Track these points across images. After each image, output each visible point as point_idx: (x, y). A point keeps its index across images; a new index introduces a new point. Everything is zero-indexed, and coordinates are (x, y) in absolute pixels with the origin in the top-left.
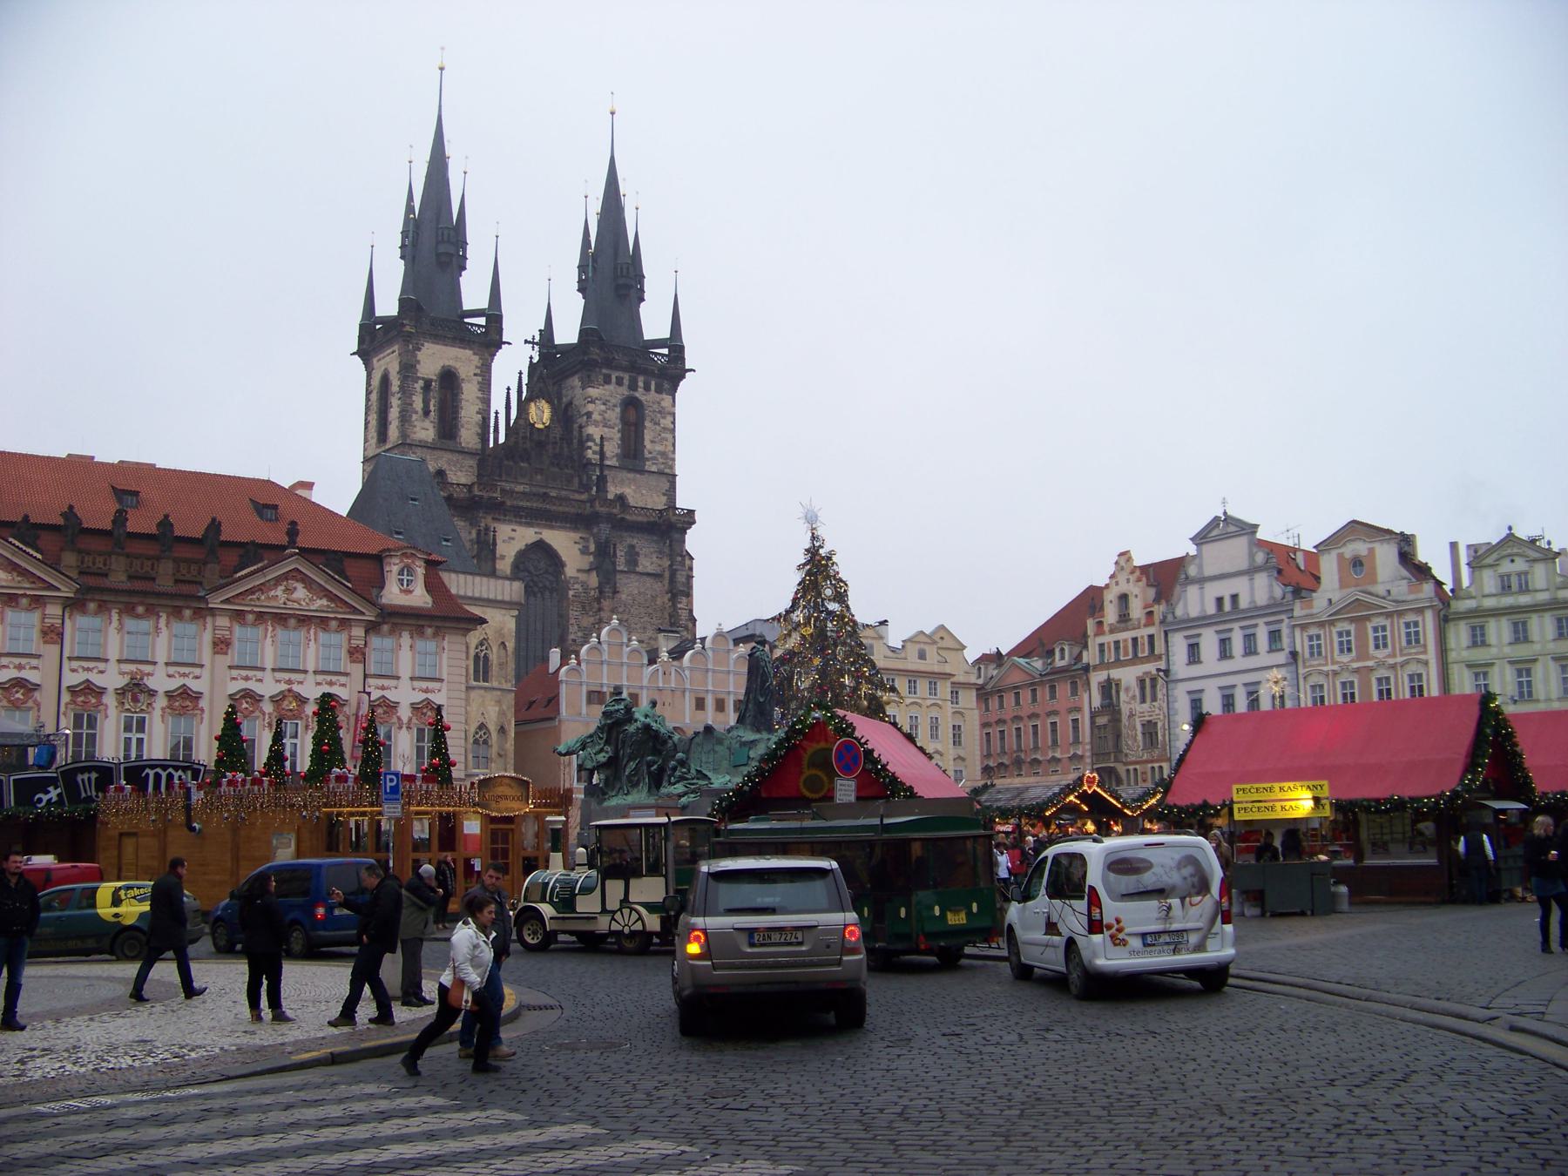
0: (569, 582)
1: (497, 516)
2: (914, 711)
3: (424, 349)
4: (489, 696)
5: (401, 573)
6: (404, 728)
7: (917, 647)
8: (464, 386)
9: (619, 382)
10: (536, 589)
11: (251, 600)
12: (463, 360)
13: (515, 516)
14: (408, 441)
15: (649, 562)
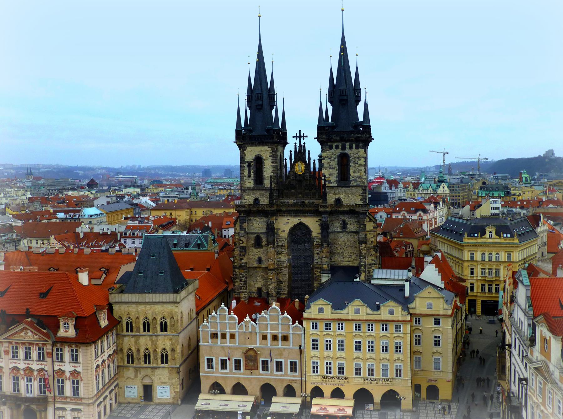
0: (314, 239)
1: (281, 215)
2: (385, 340)
3: (247, 150)
4: (166, 338)
5: (65, 324)
6: (68, 380)
7: (388, 308)
8: (265, 162)
9: (337, 147)
10: (301, 242)
11: (15, 337)
12: (265, 151)
13: (289, 214)
14: (243, 189)
15: (352, 226)
